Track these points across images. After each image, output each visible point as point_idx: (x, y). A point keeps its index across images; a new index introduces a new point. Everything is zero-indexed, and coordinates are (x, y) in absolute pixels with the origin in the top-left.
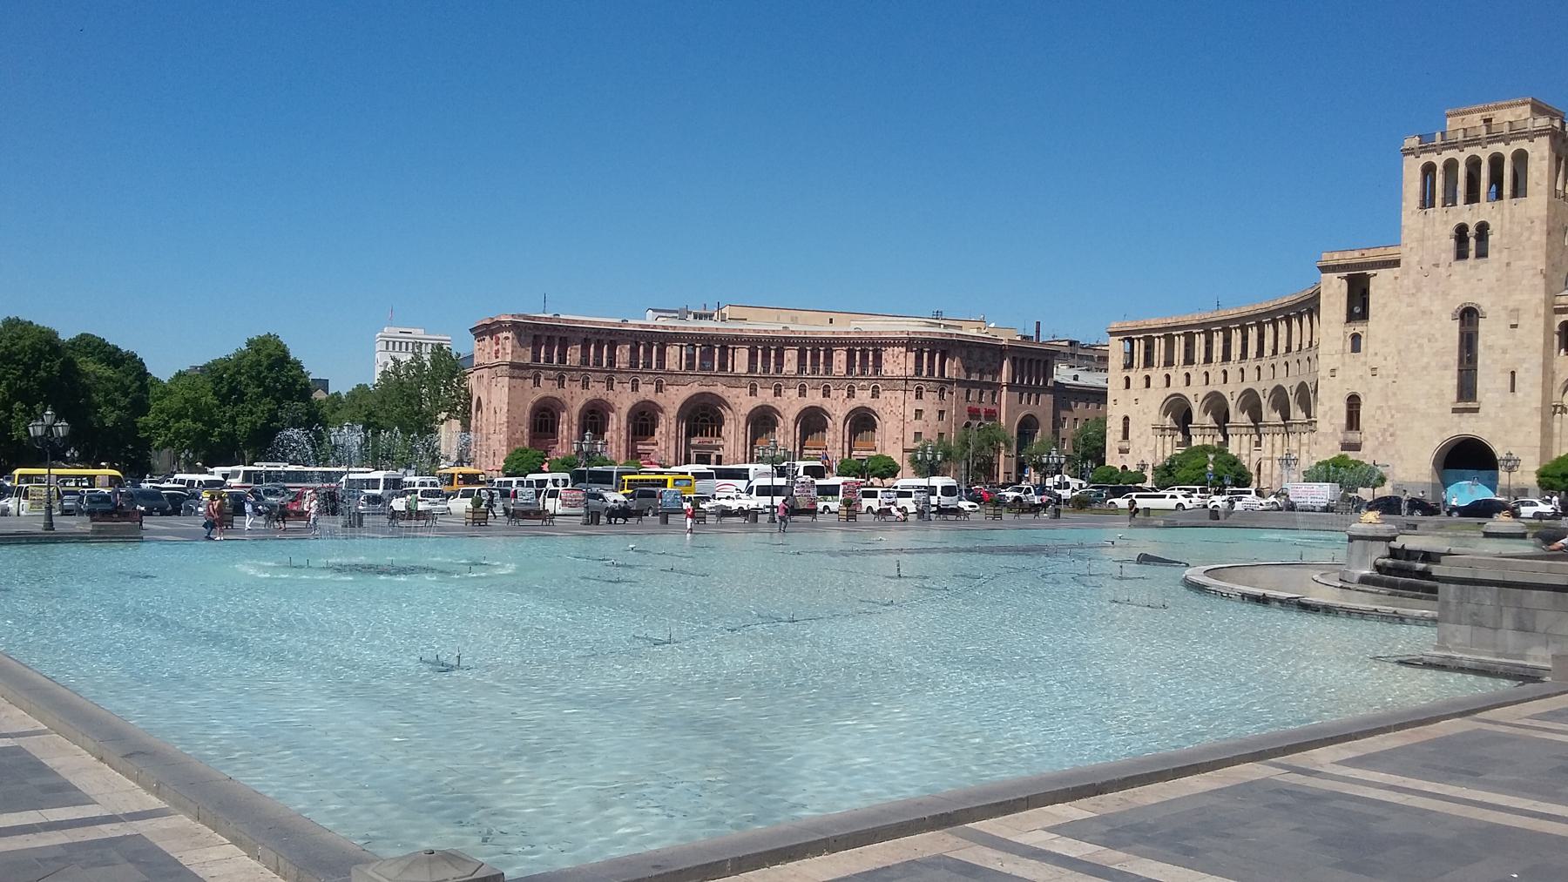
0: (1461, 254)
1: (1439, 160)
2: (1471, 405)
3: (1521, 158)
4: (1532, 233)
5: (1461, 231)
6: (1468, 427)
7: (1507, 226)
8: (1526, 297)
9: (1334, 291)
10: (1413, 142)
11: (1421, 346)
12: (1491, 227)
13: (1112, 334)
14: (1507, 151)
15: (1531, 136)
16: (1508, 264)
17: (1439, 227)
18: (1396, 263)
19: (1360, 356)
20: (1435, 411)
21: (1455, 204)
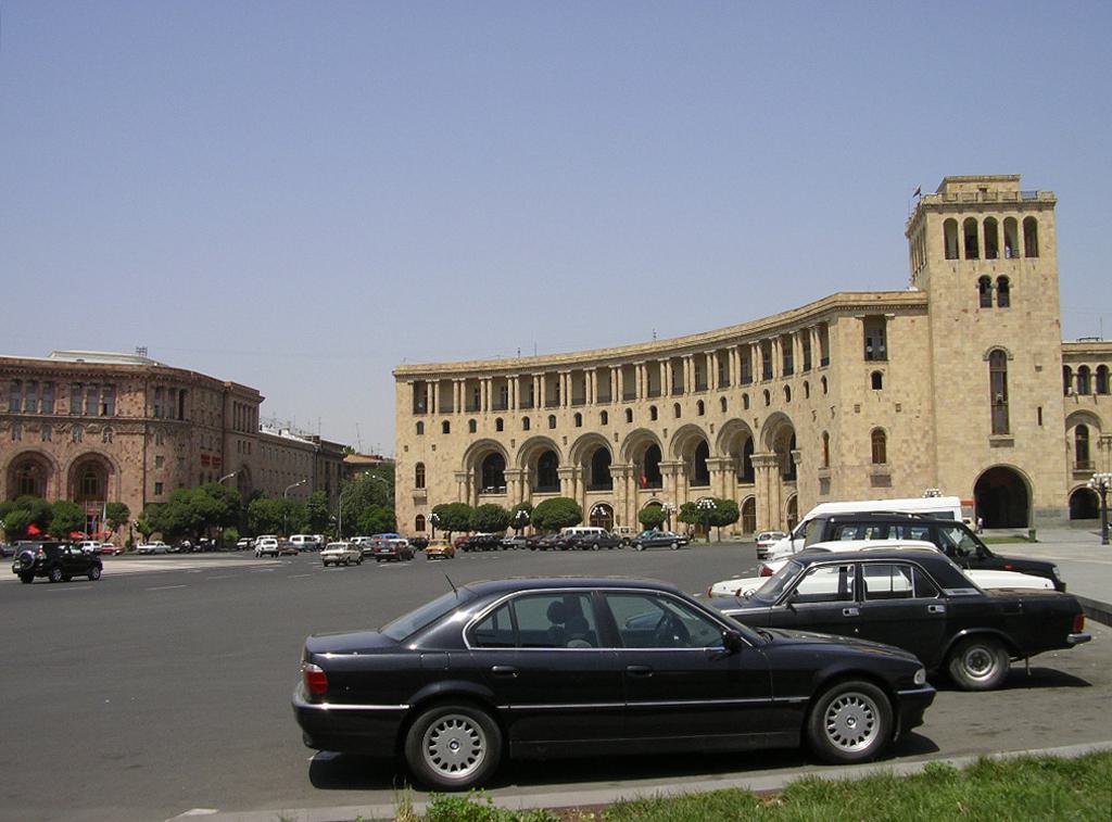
0: (986, 304)
1: (960, 218)
2: (1007, 437)
5: (984, 283)
6: (1003, 457)
7: (1025, 280)
8: (1046, 343)
9: (848, 335)
11: (955, 383)
16: (1029, 314)
17: (965, 278)
18: (922, 308)
20: (973, 442)
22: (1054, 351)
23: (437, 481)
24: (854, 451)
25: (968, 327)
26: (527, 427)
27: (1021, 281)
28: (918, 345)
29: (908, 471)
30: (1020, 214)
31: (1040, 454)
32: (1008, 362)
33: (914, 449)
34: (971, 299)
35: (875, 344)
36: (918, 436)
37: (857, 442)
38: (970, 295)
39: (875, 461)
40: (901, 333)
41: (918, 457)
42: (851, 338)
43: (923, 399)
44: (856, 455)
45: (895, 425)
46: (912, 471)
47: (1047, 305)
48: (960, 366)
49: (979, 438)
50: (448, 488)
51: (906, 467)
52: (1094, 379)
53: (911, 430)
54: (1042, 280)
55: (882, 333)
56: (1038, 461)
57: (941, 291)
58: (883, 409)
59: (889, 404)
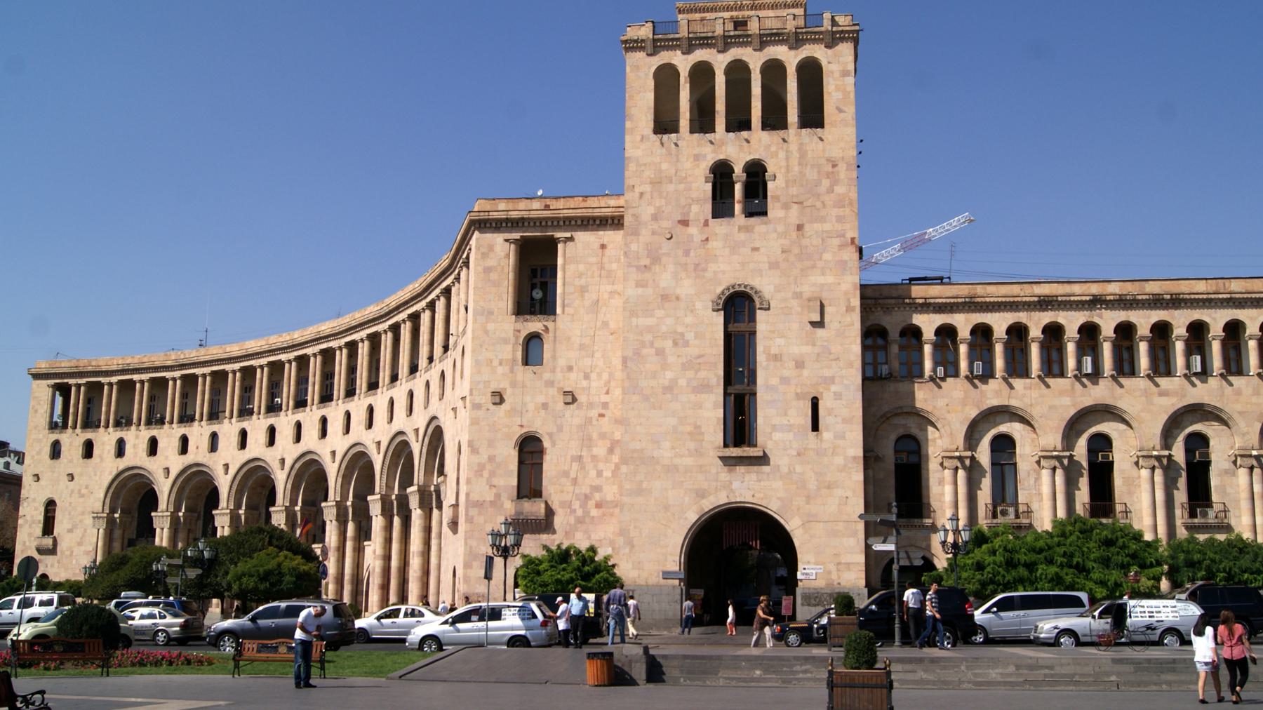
1: (683, 63)
3: (811, 74)
4: (835, 182)
5: (721, 174)
6: (747, 488)
7: (796, 169)
8: (830, 279)
10: (645, 32)
11: (660, 352)
12: (771, 169)
13: (37, 376)
14: (792, 59)
15: (832, 40)
16: (800, 227)
17: (687, 164)
18: (614, 222)
19: (545, 372)
20: (689, 461)
21: (711, 129)
22: (846, 293)
23: (70, 526)
24: (486, 474)
25: (687, 253)
26: (184, 449)
27: (788, 171)
28: (609, 288)
29: (580, 512)
30: (793, 52)
31: (812, 485)
32: (760, 315)
33: (593, 473)
34: (698, 201)
35: (535, 287)
36: (600, 450)
37: (491, 459)
38: (694, 195)
39: (520, 496)
40: (582, 267)
41: (598, 489)
42: (494, 276)
43: (613, 384)
44: (488, 481)
45: (560, 429)
46: (586, 513)
47: (835, 212)
48: (670, 321)
49: (698, 453)
50: (83, 536)
51: (576, 505)
52: (928, 349)
53: (590, 439)
54: (830, 169)
55: (551, 271)
56: (809, 499)
57: (642, 189)
58: (541, 399)
59: (553, 391)
